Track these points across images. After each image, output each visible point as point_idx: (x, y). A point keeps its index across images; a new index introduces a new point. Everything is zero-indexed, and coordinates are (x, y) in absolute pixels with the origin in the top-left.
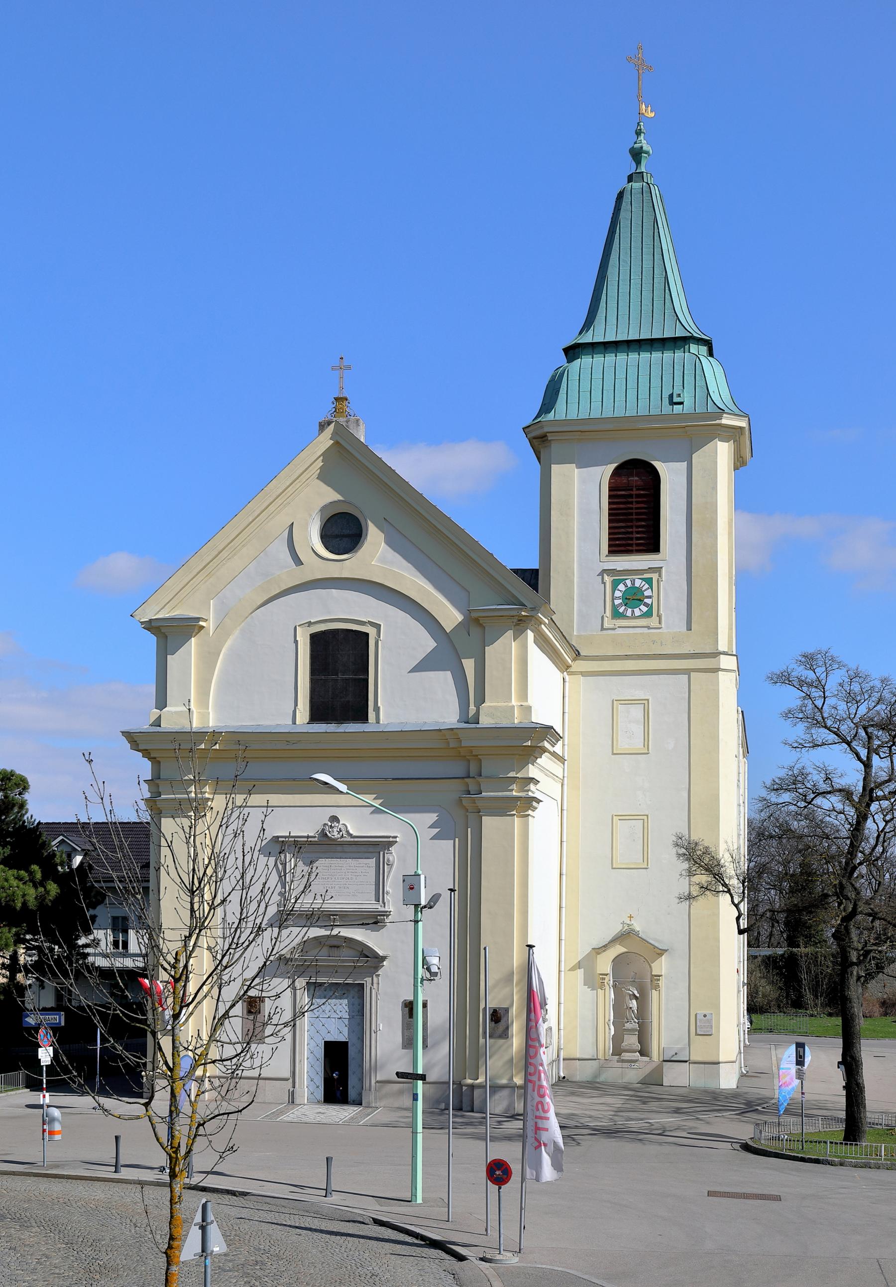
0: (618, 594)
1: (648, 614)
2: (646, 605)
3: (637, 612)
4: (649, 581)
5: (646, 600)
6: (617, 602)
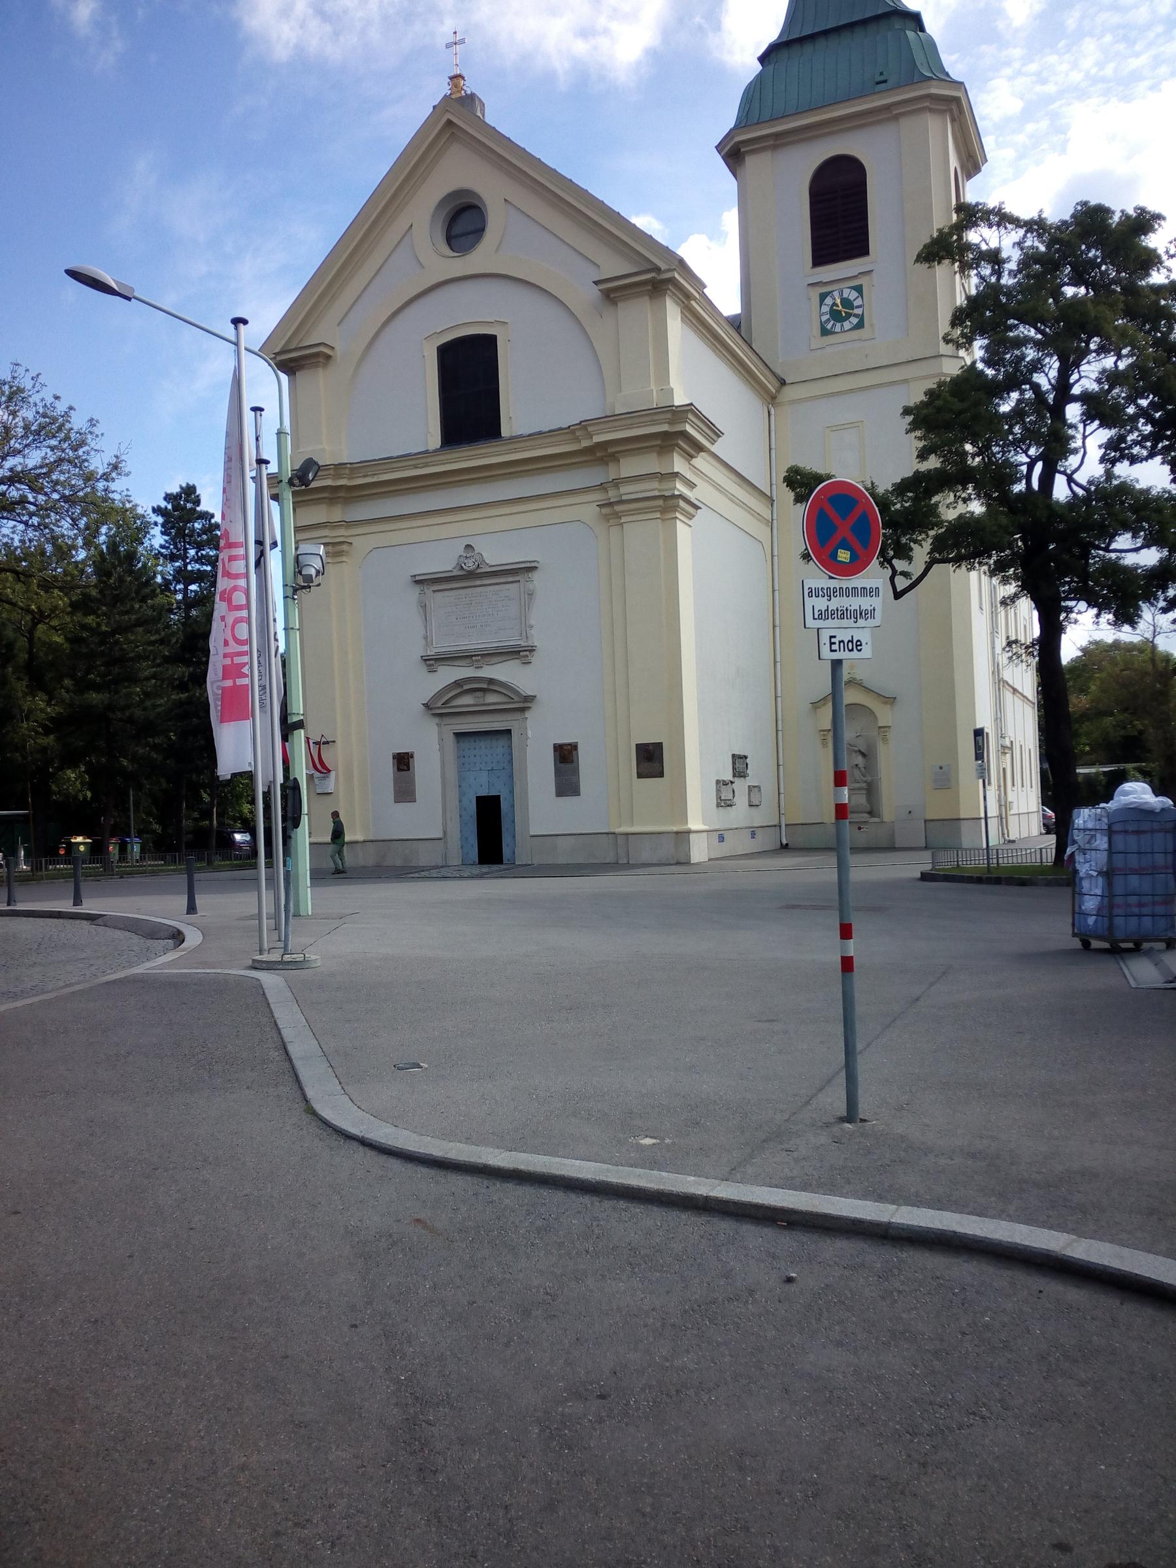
0: (825, 309)
1: (860, 325)
2: (856, 316)
4: (859, 289)
5: (858, 311)
6: (824, 318)
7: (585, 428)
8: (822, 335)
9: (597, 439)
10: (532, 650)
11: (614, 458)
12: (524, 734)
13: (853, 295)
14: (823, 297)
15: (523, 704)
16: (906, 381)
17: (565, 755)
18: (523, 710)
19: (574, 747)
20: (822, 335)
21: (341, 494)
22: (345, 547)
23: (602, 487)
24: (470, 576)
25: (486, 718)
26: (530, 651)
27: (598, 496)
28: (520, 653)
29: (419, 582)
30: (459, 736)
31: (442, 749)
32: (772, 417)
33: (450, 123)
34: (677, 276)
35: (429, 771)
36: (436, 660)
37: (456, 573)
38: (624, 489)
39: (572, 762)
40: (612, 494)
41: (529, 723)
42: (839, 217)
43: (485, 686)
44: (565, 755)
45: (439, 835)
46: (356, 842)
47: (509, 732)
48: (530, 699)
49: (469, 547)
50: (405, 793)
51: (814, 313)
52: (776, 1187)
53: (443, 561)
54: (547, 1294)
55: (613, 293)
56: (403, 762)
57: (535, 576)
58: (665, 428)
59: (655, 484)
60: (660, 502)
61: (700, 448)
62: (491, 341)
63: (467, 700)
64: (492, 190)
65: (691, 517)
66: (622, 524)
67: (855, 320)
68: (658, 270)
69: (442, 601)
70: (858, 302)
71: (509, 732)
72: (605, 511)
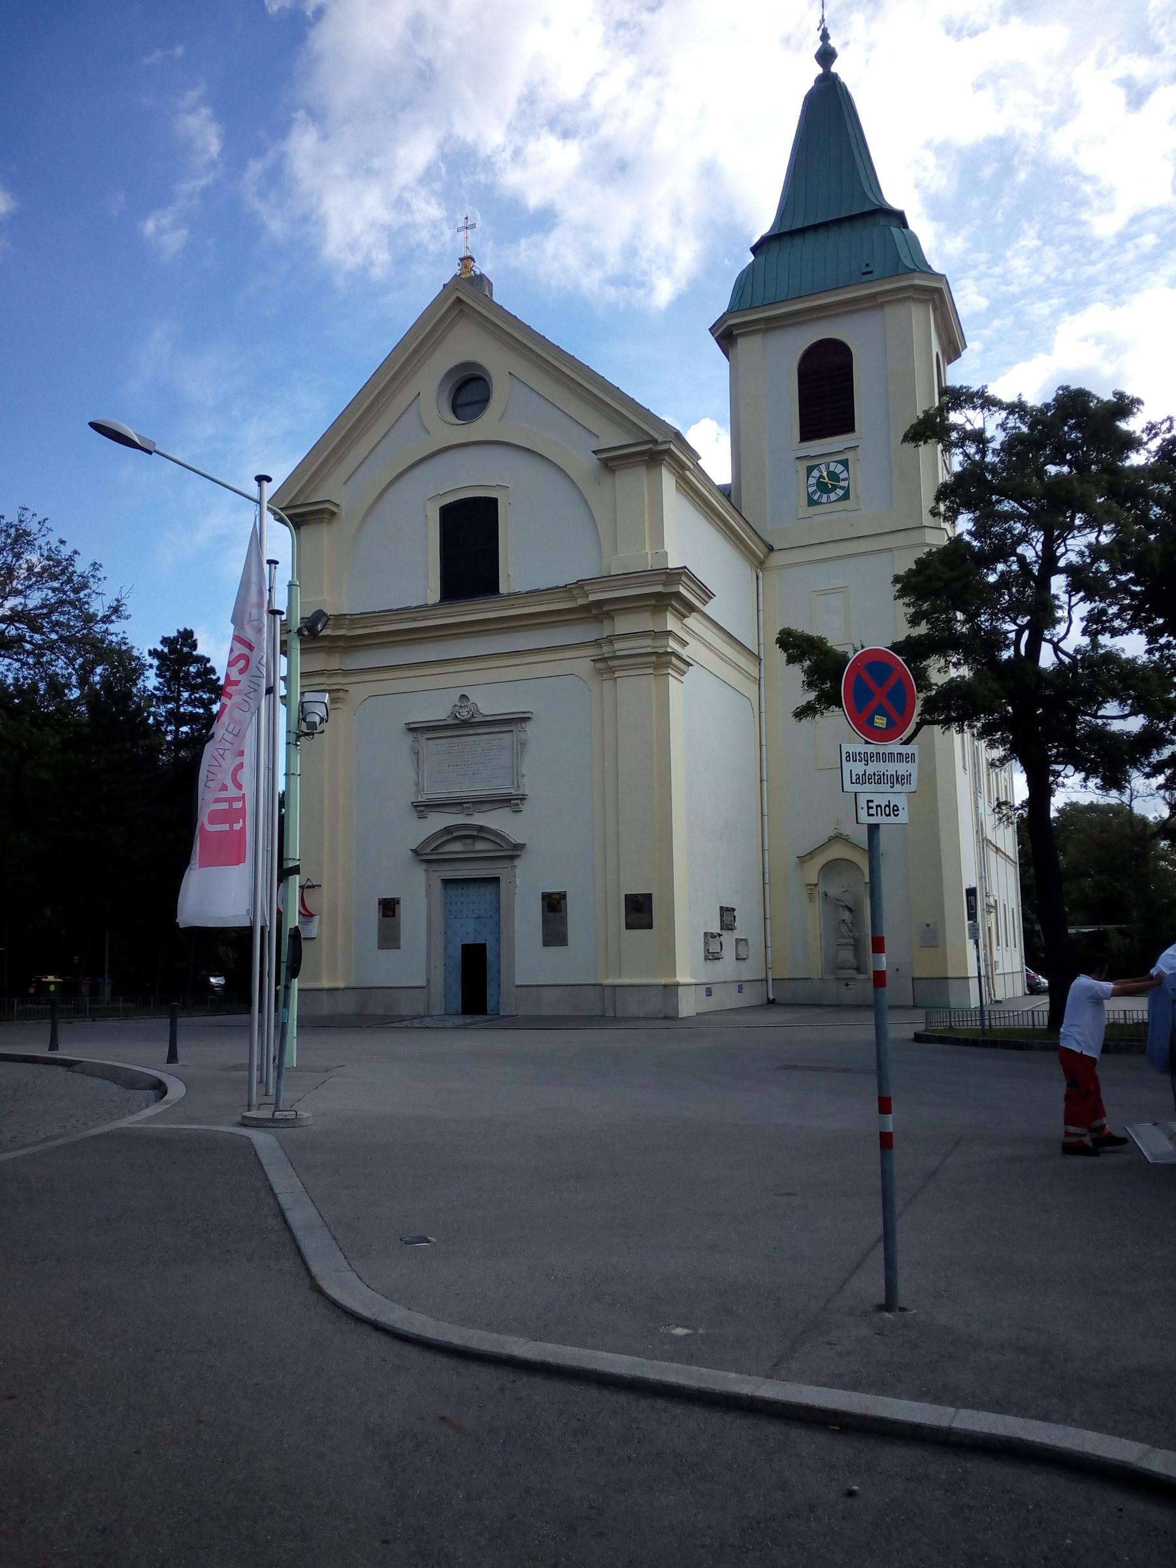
0: (812, 481)
1: (846, 497)
2: (841, 488)
3: (833, 497)
4: (845, 463)
5: (845, 484)
6: (811, 490)
7: (581, 587)
8: (809, 505)
9: (593, 598)
10: (523, 798)
11: (609, 616)
12: (512, 883)
13: (839, 468)
14: (810, 470)
15: (512, 852)
16: (890, 550)
17: (554, 904)
18: (512, 858)
19: (563, 896)
20: (809, 505)
21: (341, 644)
22: (341, 694)
23: (597, 643)
24: (464, 725)
25: (475, 865)
26: (521, 799)
27: (592, 652)
28: (511, 802)
29: (413, 729)
30: (447, 882)
31: (429, 896)
32: (761, 581)
33: (459, 301)
34: (673, 448)
35: (415, 918)
36: (426, 806)
37: (450, 721)
38: (617, 646)
39: (560, 911)
40: (606, 650)
41: (518, 871)
42: (826, 396)
43: (475, 833)
44: (554, 904)
45: (422, 983)
46: (337, 989)
47: (497, 879)
48: (519, 847)
49: (463, 696)
50: (389, 938)
51: (800, 485)
52: (825, 1385)
53: (438, 710)
54: (592, 1507)
55: (612, 462)
56: (389, 907)
57: (529, 727)
58: (659, 589)
59: (648, 642)
60: (653, 659)
61: (692, 608)
62: (492, 504)
63: (457, 847)
64: (497, 363)
65: (683, 673)
66: (615, 679)
67: (840, 492)
68: (655, 441)
69: (433, 748)
70: (844, 475)
71: (497, 879)
72: (599, 665)
